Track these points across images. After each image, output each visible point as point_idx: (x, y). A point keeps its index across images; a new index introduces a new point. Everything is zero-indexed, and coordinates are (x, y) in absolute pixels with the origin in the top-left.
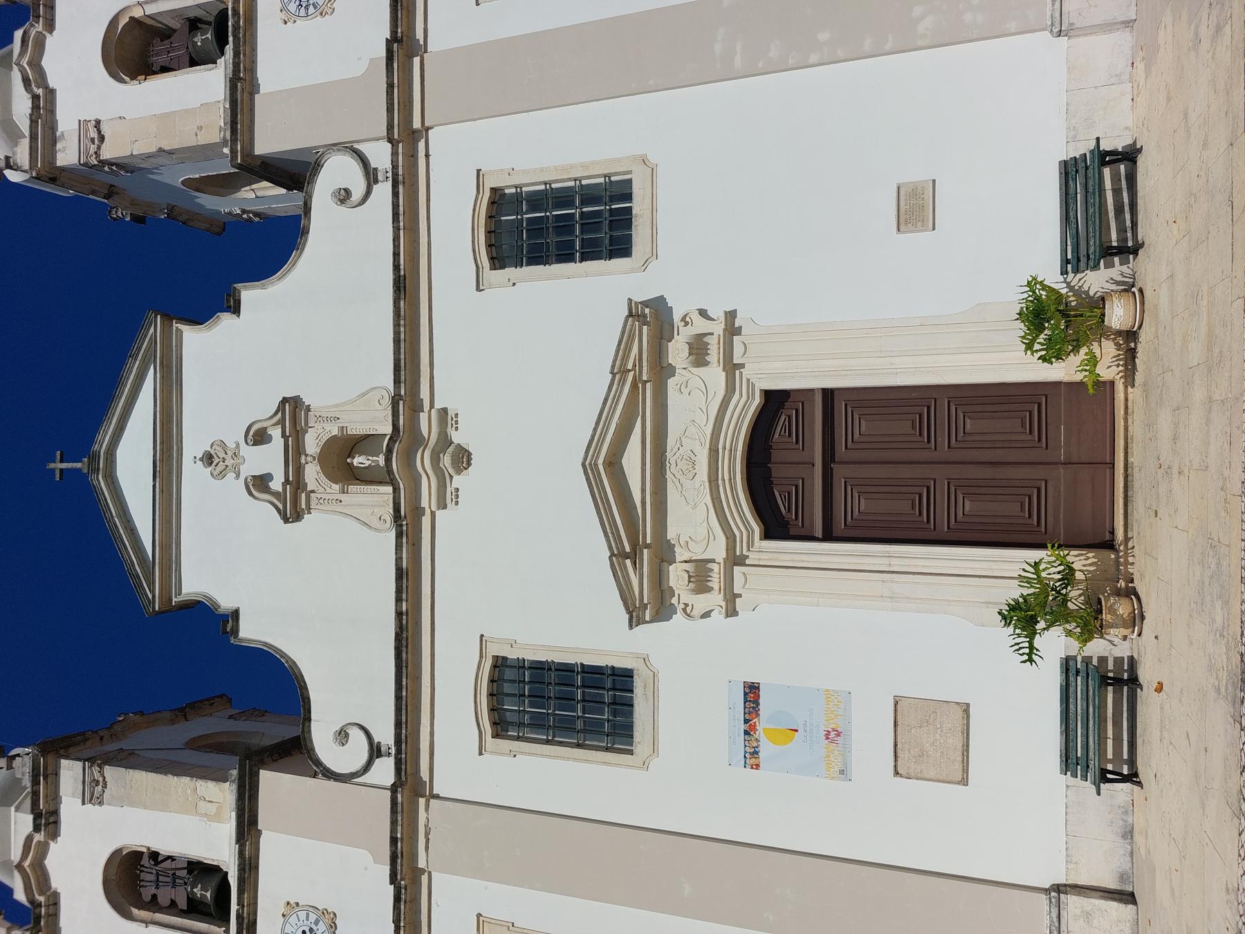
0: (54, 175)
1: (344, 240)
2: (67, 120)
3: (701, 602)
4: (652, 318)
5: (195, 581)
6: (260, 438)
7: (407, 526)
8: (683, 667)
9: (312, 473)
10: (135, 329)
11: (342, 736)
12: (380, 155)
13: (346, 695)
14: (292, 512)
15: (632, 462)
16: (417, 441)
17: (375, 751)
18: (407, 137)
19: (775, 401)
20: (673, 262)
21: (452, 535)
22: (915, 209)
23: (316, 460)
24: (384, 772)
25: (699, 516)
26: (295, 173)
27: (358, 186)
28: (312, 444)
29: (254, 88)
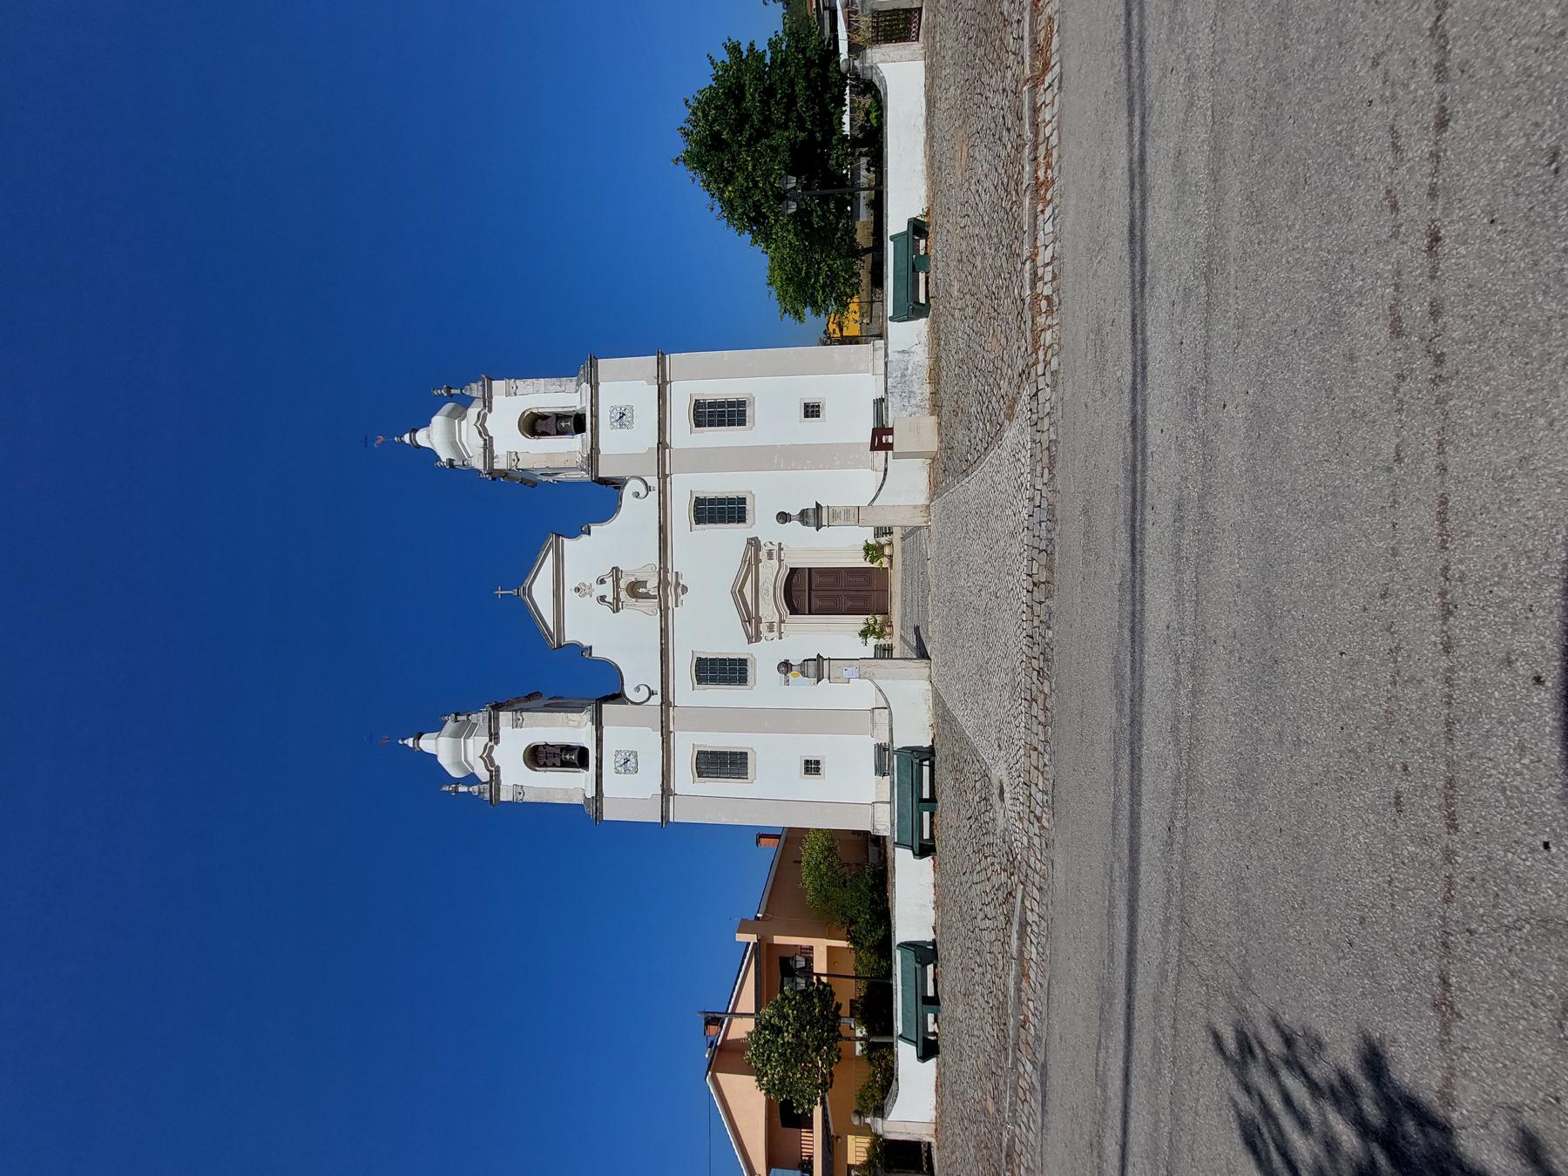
0: (492, 472)
1: (636, 510)
2: (499, 449)
3: (771, 635)
4: (754, 543)
5: (570, 636)
6: (602, 582)
7: (664, 612)
8: (763, 657)
9: (623, 595)
10: (546, 538)
11: (638, 689)
12: (653, 481)
13: (638, 675)
15: (748, 591)
16: (667, 583)
17: (652, 693)
18: (663, 477)
19: (793, 571)
21: (680, 617)
25: (770, 608)
26: (616, 485)
27: (643, 492)
28: (623, 584)
29: (598, 452)
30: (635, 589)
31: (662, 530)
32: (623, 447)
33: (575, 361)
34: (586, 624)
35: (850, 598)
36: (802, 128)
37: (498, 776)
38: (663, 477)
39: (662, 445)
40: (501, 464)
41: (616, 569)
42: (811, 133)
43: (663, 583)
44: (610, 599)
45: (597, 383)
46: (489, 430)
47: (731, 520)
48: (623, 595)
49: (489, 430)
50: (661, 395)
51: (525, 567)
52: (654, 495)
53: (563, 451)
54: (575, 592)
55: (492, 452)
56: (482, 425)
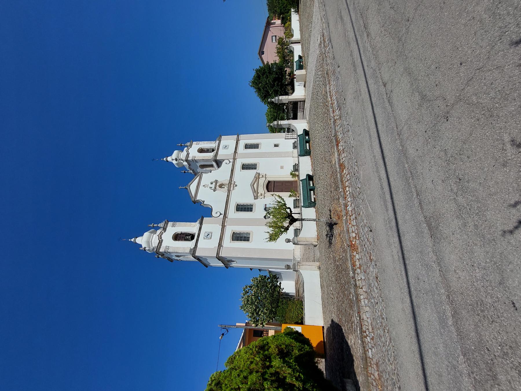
1: (226, 167)
3: (261, 197)
5: (198, 198)
7: (229, 191)
9: (217, 187)
11: (217, 213)
12: (232, 160)
13: (218, 208)
14: (214, 191)
15: (255, 186)
17: (221, 214)
18: (234, 159)
19: (269, 182)
20: (260, 170)
21: (233, 193)
22: (282, 167)
23: (218, 185)
24: (222, 216)
25: (262, 190)
27: (228, 162)
28: (218, 184)
31: (232, 170)
33: (216, 136)
37: (161, 243)
38: (234, 159)
44: (213, 188)
52: (231, 164)
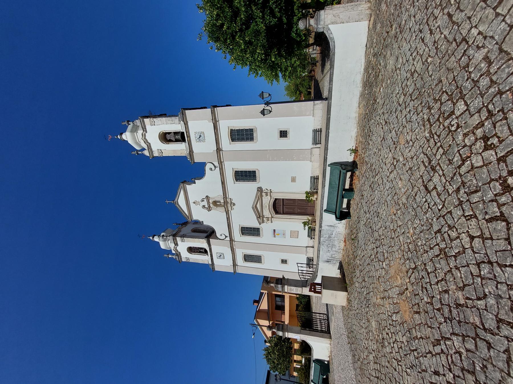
0: (154, 157)
1: (211, 176)
2: (154, 148)
4: (260, 190)
6: (203, 201)
8: (266, 228)
9: (211, 205)
10: (179, 186)
11: (221, 235)
12: (216, 164)
13: (221, 230)
15: (258, 206)
16: (227, 202)
18: (221, 163)
20: (263, 182)
21: (234, 214)
22: (293, 180)
23: (211, 204)
24: (228, 239)
25: (267, 213)
28: (211, 201)
29: (193, 152)
30: (215, 203)
31: (223, 183)
32: (202, 150)
33: (175, 109)
34: (199, 214)
35: (299, 209)
36: (274, 16)
38: (221, 163)
39: (219, 150)
40: (156, 154)
41: (207, 197)
42: (280, 19)
43: (226, 203)
44: (207, 206)
45: (187, 122)
46: (148, 136)
47: (249, 180)
48: (211, 205)
49: (148, 136)
50: (215, 127)
51: (174, 195)
52: (218, 169)
53: (177, 149)
54: (194, 199)
55: (151, 150)
56: (145, 138)
